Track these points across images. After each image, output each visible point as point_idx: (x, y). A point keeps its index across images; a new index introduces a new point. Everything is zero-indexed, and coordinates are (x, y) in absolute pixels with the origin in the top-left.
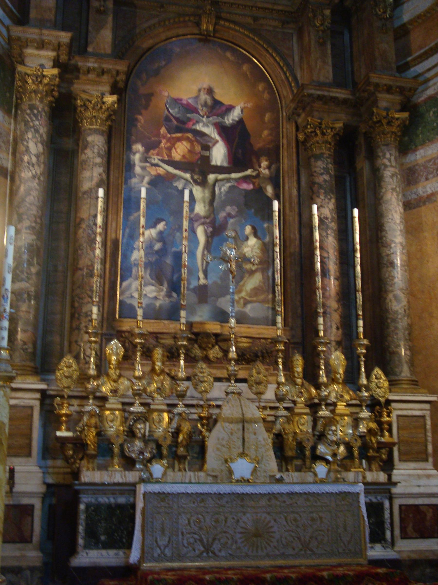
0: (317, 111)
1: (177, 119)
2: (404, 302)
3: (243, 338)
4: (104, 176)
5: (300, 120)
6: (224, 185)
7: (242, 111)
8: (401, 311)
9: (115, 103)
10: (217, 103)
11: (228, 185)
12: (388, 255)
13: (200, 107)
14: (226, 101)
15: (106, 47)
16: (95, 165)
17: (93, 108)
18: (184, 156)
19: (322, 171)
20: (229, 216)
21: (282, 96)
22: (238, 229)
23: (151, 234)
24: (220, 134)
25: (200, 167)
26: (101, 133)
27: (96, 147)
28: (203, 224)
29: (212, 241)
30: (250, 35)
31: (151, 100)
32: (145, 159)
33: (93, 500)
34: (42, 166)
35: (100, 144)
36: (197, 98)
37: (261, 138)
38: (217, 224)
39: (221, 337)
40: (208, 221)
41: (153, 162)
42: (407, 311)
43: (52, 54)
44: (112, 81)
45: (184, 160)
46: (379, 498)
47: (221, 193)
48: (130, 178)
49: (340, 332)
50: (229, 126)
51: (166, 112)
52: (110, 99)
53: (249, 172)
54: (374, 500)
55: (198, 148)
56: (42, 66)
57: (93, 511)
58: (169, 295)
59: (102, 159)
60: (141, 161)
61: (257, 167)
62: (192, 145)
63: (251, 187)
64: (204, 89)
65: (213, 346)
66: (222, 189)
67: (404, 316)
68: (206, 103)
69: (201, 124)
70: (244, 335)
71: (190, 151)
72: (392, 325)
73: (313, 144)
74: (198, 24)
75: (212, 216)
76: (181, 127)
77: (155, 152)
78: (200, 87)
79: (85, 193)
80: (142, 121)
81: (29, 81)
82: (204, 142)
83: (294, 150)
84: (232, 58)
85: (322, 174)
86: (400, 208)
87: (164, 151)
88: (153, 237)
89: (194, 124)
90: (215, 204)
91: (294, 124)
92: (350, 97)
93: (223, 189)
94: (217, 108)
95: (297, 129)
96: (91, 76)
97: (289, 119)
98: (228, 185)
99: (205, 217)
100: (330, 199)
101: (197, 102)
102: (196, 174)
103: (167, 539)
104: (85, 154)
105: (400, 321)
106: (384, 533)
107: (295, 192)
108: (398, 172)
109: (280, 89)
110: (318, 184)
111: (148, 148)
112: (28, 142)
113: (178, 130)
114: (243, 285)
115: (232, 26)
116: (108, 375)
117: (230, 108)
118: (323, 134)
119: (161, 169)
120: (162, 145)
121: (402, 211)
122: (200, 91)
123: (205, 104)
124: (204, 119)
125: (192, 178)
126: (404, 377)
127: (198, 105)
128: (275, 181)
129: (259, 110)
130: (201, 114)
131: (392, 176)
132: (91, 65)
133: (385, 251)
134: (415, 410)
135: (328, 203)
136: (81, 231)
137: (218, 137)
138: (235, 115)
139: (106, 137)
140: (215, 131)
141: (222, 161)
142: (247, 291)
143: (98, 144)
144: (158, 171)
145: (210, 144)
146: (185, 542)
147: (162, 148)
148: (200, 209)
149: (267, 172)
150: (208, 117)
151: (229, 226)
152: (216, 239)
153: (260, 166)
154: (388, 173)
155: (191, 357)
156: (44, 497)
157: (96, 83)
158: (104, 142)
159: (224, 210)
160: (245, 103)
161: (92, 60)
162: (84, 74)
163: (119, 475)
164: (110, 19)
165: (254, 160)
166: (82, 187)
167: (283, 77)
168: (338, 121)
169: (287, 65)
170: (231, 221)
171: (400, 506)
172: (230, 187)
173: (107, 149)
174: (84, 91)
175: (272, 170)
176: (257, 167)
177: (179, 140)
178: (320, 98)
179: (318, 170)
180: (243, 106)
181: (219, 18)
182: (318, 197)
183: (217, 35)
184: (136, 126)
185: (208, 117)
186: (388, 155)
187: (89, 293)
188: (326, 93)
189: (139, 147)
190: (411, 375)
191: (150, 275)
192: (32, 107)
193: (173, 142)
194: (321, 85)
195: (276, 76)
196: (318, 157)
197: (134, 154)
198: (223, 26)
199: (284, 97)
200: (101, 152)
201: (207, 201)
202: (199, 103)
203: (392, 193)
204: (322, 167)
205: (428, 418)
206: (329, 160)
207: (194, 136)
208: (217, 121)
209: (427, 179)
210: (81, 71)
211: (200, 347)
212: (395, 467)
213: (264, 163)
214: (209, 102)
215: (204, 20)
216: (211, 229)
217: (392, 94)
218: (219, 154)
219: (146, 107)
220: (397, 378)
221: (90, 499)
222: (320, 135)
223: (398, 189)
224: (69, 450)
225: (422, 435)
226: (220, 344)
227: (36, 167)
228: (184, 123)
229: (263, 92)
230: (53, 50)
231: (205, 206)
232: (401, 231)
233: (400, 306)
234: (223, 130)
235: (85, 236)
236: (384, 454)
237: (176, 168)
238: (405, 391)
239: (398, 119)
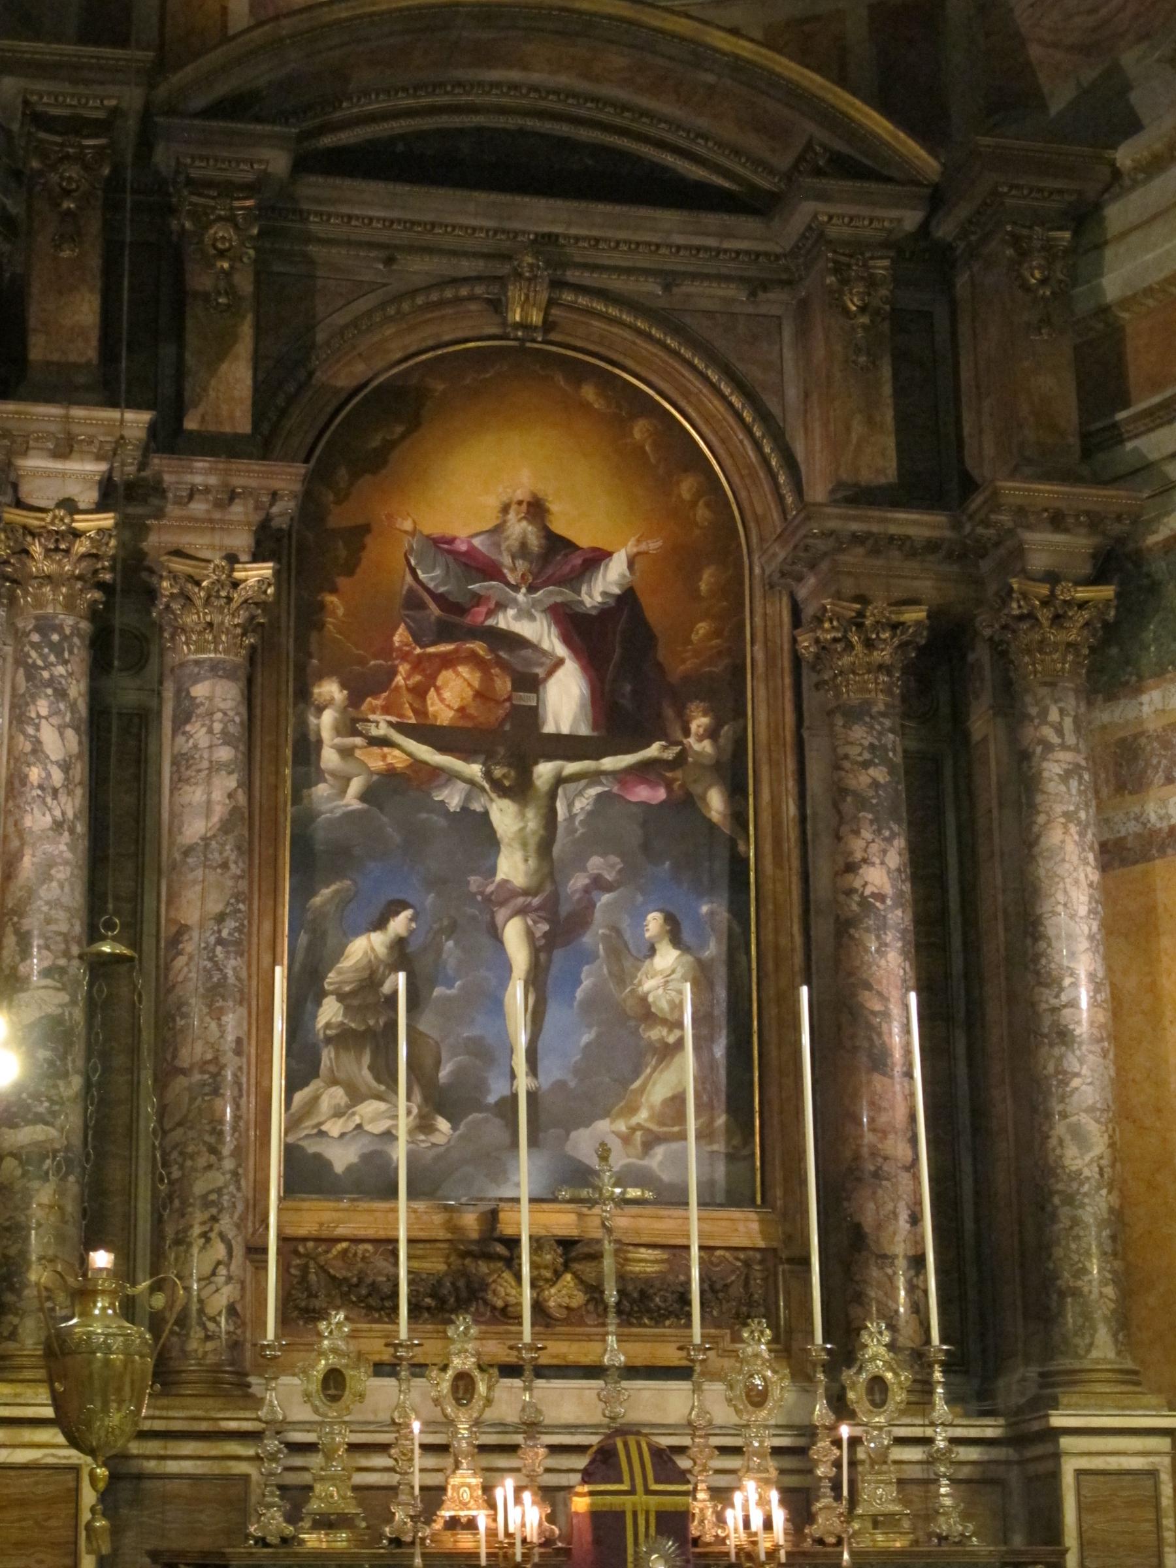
0: (849, 573)
1: (439, 599)
2: (1099, 1145)
3: (643, 1250)
4: (241, 798)
5: (802, 592)
6: (580, 793)
7: (631, 565)
8: (1091, 1172)
9: (269, 585)
10: (556, 544)
11: (593, 791)
12: (1055, 1010)
13: (507, 560)
14: (584, 539)
15: (238, 414)
16: (215, 767)
17: (207, 602)
18: (462, 710)
19: (867, 756)
20: (598, 884)
21: (749, 515)
22: (625, 924)
23: (373, 949)
24: (567, 640)
25: (510, 742)
26: (230, 674)
27: (219, 715)
28: (522, 911)
29: (550, 961)
30: (653, 331)
31: (363, 547)
32: (350, 725)
34: (79, 792)
35: (229, 704)
36: (497, 530)
37: (689, 645)
38: (564, 909)
39: (581, 1249)
40: (536, 901)
41: (374, 732)
42: (1107, 1170)
43: (97, 468)
44: (257, 518)
45: (461, 723)
47: (571, 817)
48: (310, 784)
50: (594, 612)
51: (409, 578)
52: (256, 574)
53: (654, 750)
55: (503, 685)
56: (69, 505)
59: (236, 748)
60: (338, 731)
61: (679, 735)
62: (487, 678)
63: (661, 794)
64: (520, 503)
65: (558, 1275)
66: (578, 804)
67: (1099, 1188)
68: (524, 545)
69: (511, 612)
70: (645, 1239)
71: (478, 694)
72: (1064, 1212)
73: (841, 673)
74: (497, 306)
75: (548, 888)
76: (454, 621)
78: (505, 499)
79: (188, 851)
80: (340, 612)
81: (37, 549)
82: (519, 668)
83: (788, 681)
84: (598, 405)
85: (866, 765)
86: (1089, 869)
87: (406, 698)
88: (376, 957)
89: (491, 613)
91: (785, 600)
92: (948, 534)
93: (578, 805)
94: (560, 561)
95: (797, 622)
96: (199, 507)
97: (772, 587)
98: (593, 791)
99: (526, 892)
100: (889, 840)
101: (498, 545)
102: (498, 764)
104: (189, 736)
105: (1086, 1200)
107: (792, 810)
108: (1083, 763)
109: (743, 494)
110: (855, 794)
112: (38, 729)
113: (445, 632)
114: (642, 1090)
115: (600, 307)
117: (597, 558)
118: (869, 645)
119: (397, 752)
120: (399, 680)
121: (1095, 876)
122: (505, 509)
123: (523, 550)
124: (521, 597)
125: (488, 774)
126: (1097, 1361)
127: (500, 553)
128: (733, 774)
129: (682, 561)
130: (511, 579)
131: (1065, 777)
132: (198, 479)
133: (1047, 998)
134: (1131, 1456)
135: (885, 852)
136: (181, 961)
137: (561, 650)
138: (612, 577)
139: (242, 684)
140: (554, 631)
141: (575, 721)
142: (651, 1108)
143: (222, 706)
144: (389, 760)
145: (540, 671)
147: (398, 688)
148: (512, 867)
149: (706, 747)
150: (532, 589)
151: (598, 915)
152: (558, 954)
153: (687, 732)
154: (1053, 768)
155: (494, 1308)
157: (210, 525)
158: (239, 698)
159: (584, 869)
160: (639, 541)
161: (200, 464)
162: (179, 502)
164: (246, 329)
165: (669, 712)
166: (181, 833)
167: (751, 453)
168: (914, 599)
169: (764, 416)
170: (606, 898)
172: (599, 796)
173: (246, 717)
174: (178, 553)
175: (722, 741)
176: (679, 735)
177: (448, 662)
178: (857, 539)
179: (854, 751)
180: (635, 550)
181: (557, 284)
182: (857, 833)
183: (553, 336)
184: (320, 626)
185: (532, 589)
186: (1054, 715)
187: (212, 1140)
189: (331, 690)
190: (1119, 1353)
191: (370, 1068)
192: (45, 626)
193: (429, 671)
194: (859, 496)
195: (732, 456)
196: (854, 714)
197: (320, 710)
198: (570, 307)
199: (758, 520)
200: (232, 729)
201: (533, 842)
202: (503, 547)
203: (1065, 826)
204: (866, 743)
205: (1165, 1477)
206: (887, 723)
207: (492, 650)
208: (559, 599)
210: (170, 495)
213: (700, 722)
215: (515, 293)
216: (545, 927)
217: (1066, 531)
218: (565, 700)
219: (350, 569)
220: (1077, 1365)
222: (859, 648)
223: (1082, 815)
225: (1147, 1526)
226: (576, 1266)
227: (63, 798)
228: (460, 609)
229: (694, 504)
230: (99, 458)
231: (526, 860)
232: (1091, 937)
233: (1087, 1159)
234: (579, 628)
235: (193, 975)
237: (442, 749)
238: (1100, 1403)
239: (1082, 605)
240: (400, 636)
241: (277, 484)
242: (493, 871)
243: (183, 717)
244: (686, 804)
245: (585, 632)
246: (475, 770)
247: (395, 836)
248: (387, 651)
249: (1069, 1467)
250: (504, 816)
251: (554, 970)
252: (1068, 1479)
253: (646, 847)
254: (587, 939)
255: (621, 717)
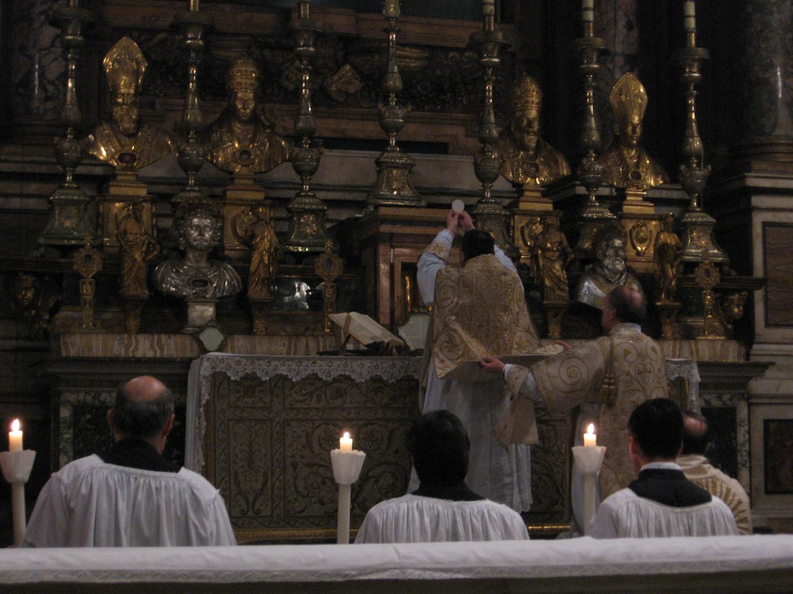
33: (89, 398)
46: (726, 397)
49: (635, 33)
54: (715, 403)
57: (89, 421)
65: (339, 66)
103: (261, 478)
105: (774, 9)
116: (111, 120)
146: (301, 484)
163: (148, 344)
171: (767, 422)
212: (757, 339)
221: (81, 396)
224: (27, 289)
236: (738, 306)
249: (758, 219)
252: (757, 229)
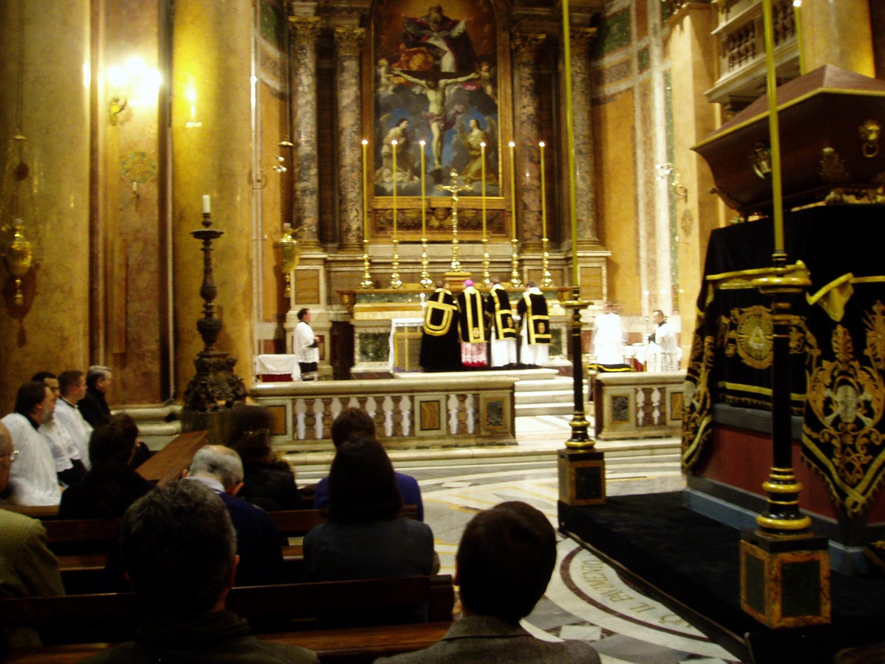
1: (413, 35)
5: (513, 31)
10: (445, 19)
11: (456, 87)
16: (351, 84)
18: (420, 67)
20: (458, 113)
24: (448, 46)
28: (437, 120)
32: (389, 71)
36: (428, 16)
38: (449, 119)
52: (359, 31)
53: (472, 76)
55: (430, 59)
58: (411, 179)
62: (426, 57)
66: (451, 92)
76: (417, 41)
77: (396, 65)
90: (446, 104)
94: (445, 24)
96: (344, 13)
98: (456, 87)
99: (439, 115)
106: (561, 349)
111: (392, 61)
113: (414, 45)
117: (456, 23)
122: (431, 9)
123: (436, 22)
125: (427, 84)
138: (461, 27)
148: (434, 109)
152: (447, 132)
156: (331, 331)
170: (459, 117)
172: (458, 90)
177: (415, 53)
188: (531, 12)
193: (410, 55)
197: (381, 67)
201: (439, 103)
209: (611, 82)
211: (437, 218)
213: (485, 68)
214: (439, 19)
218: (448, 62)
237: (415, 77)
240: (402, 46)
241: (365, 6)
242: (427, 110)
243: (343, 71)
244: (481, 90)
245: (453, 44)
246: (423, 82)
247: (402, 101)
248: (398, 50)
250: (432, 95)
251: (446, 136)
253: (470, 102)
254: (454, 128)
255: (464, 66)
